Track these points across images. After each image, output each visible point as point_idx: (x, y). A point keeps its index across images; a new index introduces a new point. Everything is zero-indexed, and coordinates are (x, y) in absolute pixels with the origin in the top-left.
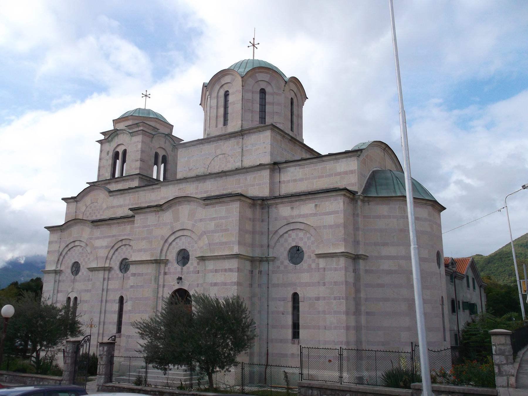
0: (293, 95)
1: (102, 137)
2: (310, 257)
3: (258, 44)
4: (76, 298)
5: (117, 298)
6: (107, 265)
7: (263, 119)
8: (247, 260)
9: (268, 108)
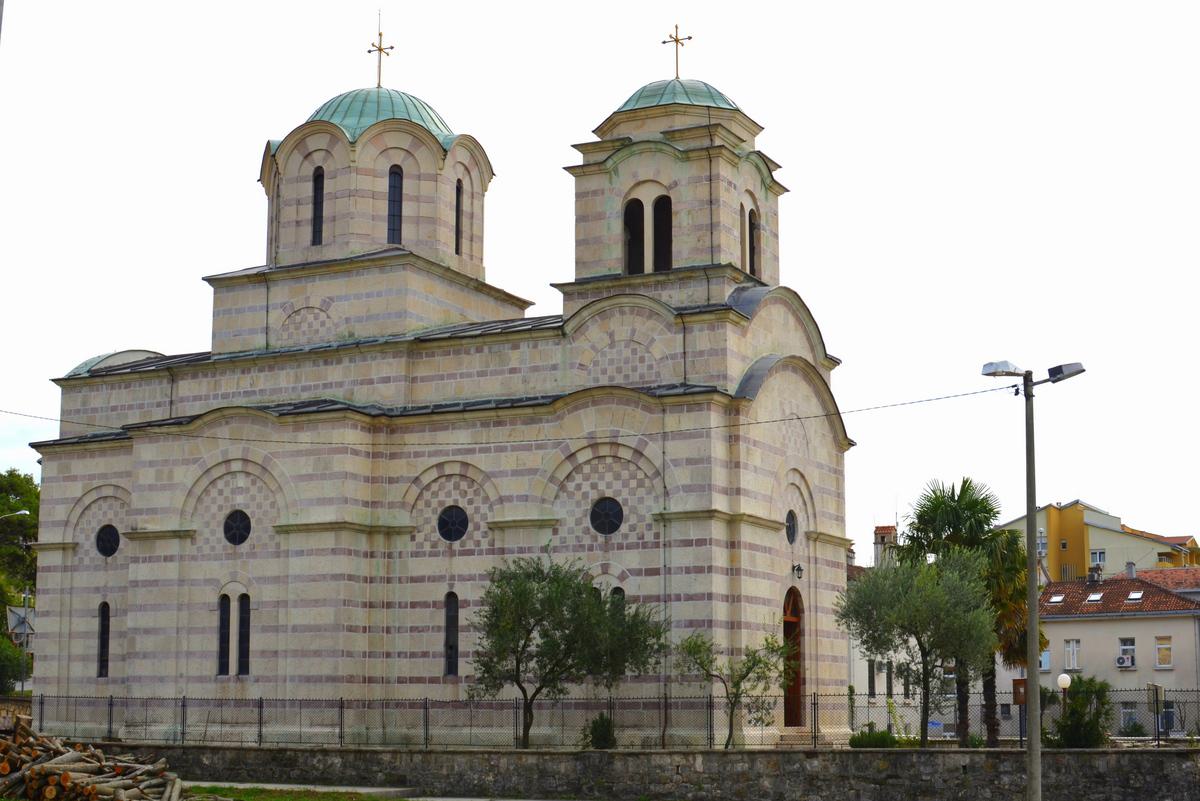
0: (460, 173)
1: (578, 159)
2: (477, 527)
3: (370, 52)
4: (244, 599)
5: (214, 599)
6: (69, 540)
7: (395, 233)
8: (362, 531)
9: (407, 209)
